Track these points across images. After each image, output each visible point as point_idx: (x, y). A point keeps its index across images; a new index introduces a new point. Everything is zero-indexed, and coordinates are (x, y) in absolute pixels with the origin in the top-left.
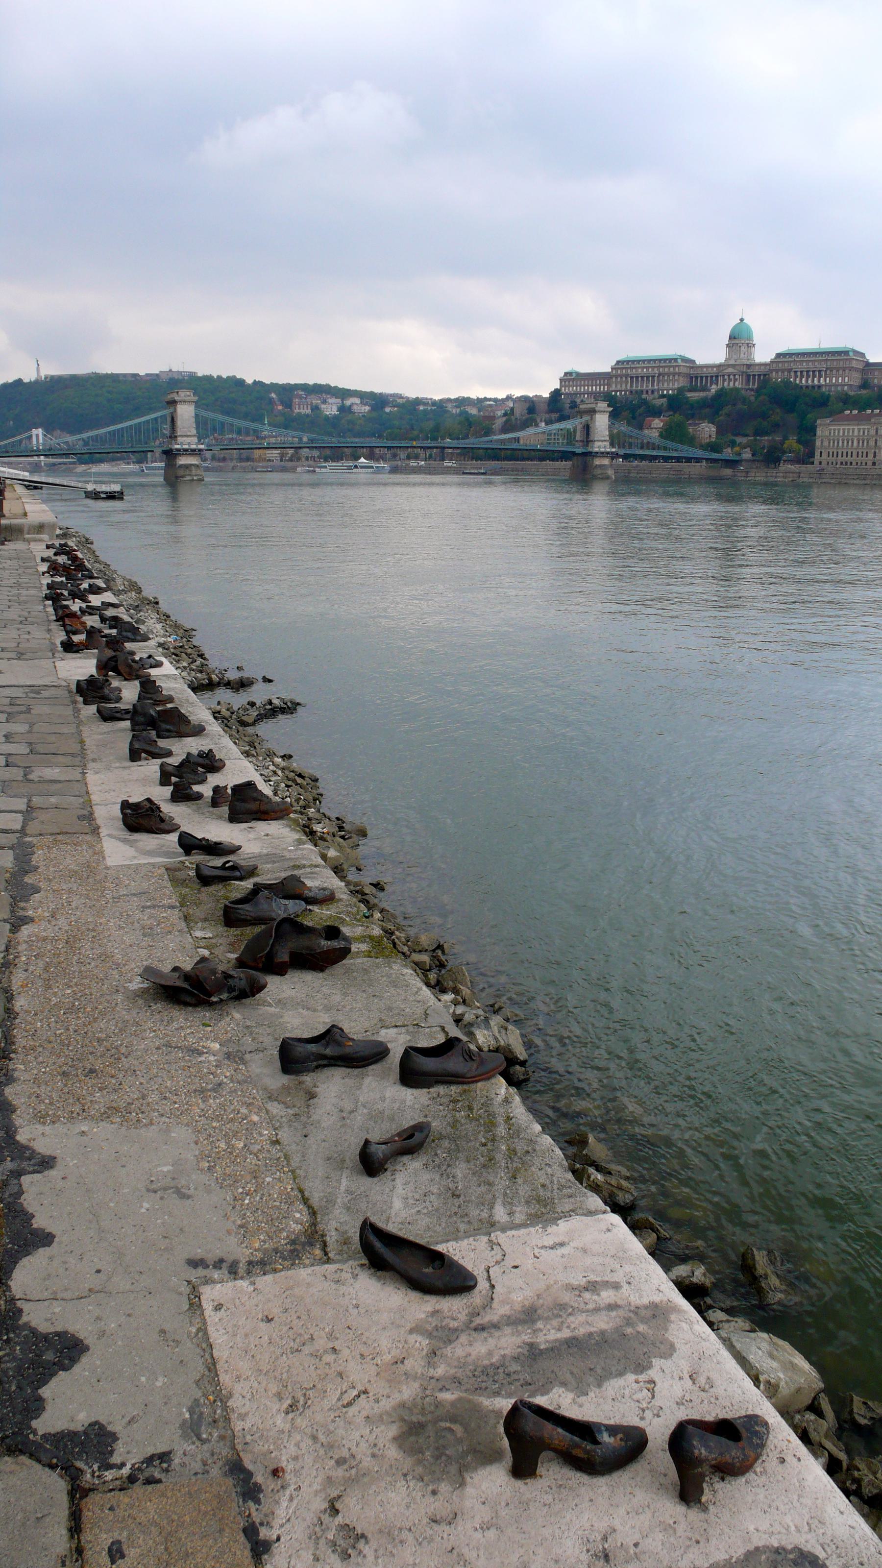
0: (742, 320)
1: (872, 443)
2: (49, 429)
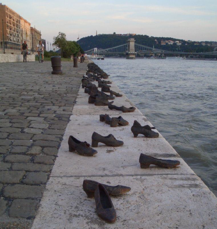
2: (98, 48)
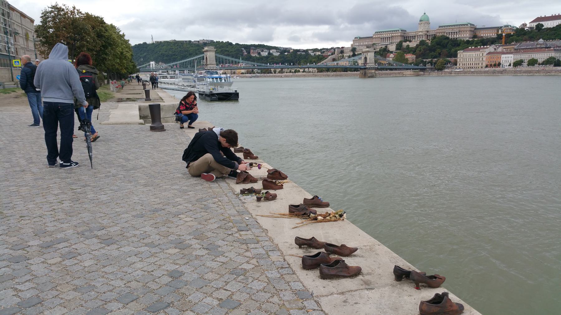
0: (425, 14)
1: (481, 59)
2: (157, 62)
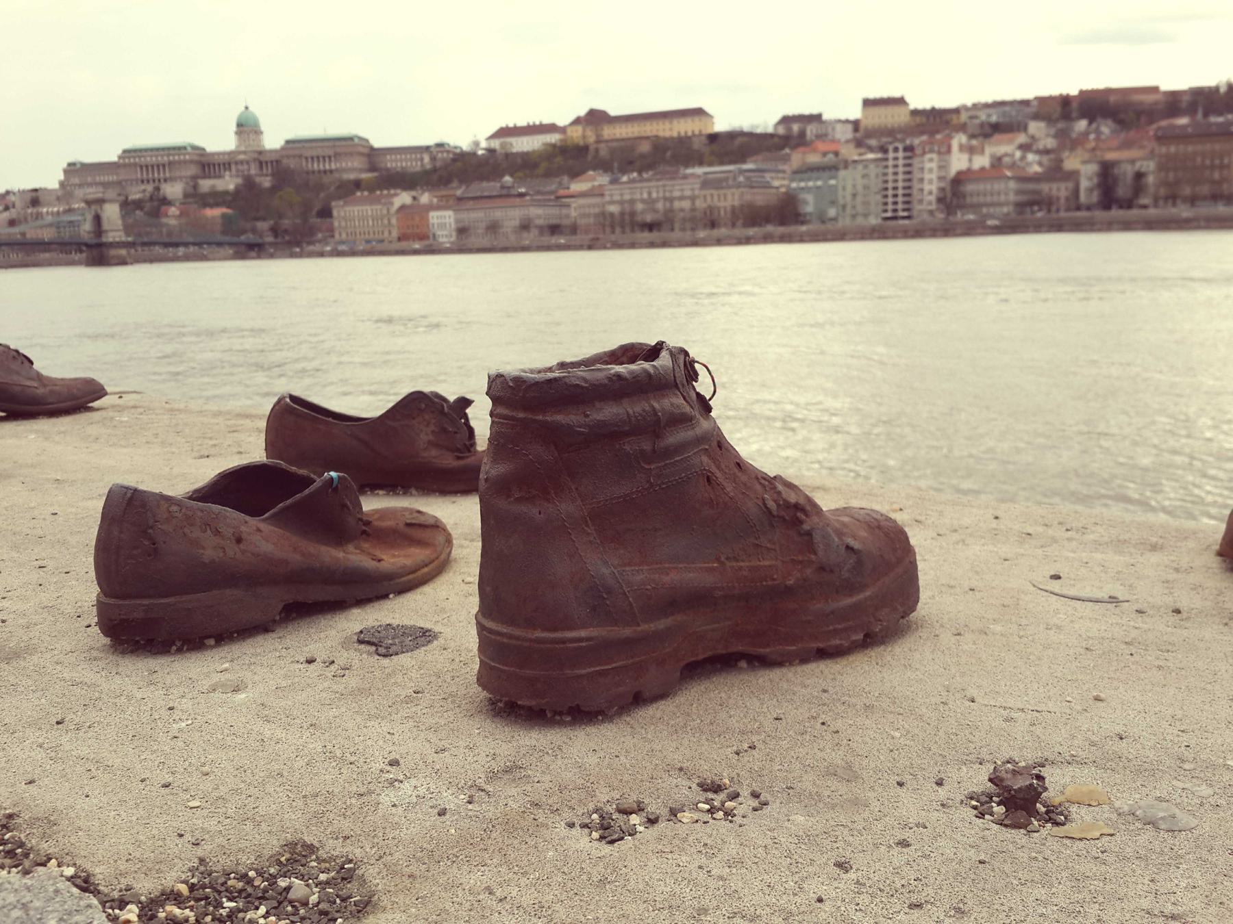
0: (247, 108)
1: (386, 222)
